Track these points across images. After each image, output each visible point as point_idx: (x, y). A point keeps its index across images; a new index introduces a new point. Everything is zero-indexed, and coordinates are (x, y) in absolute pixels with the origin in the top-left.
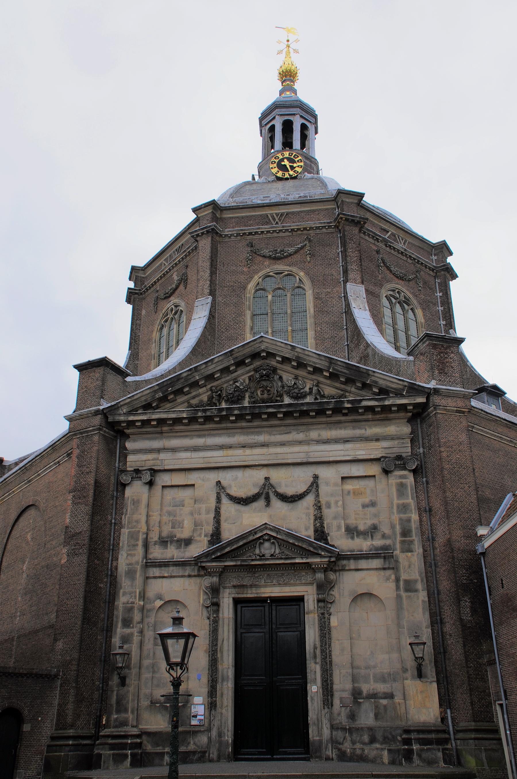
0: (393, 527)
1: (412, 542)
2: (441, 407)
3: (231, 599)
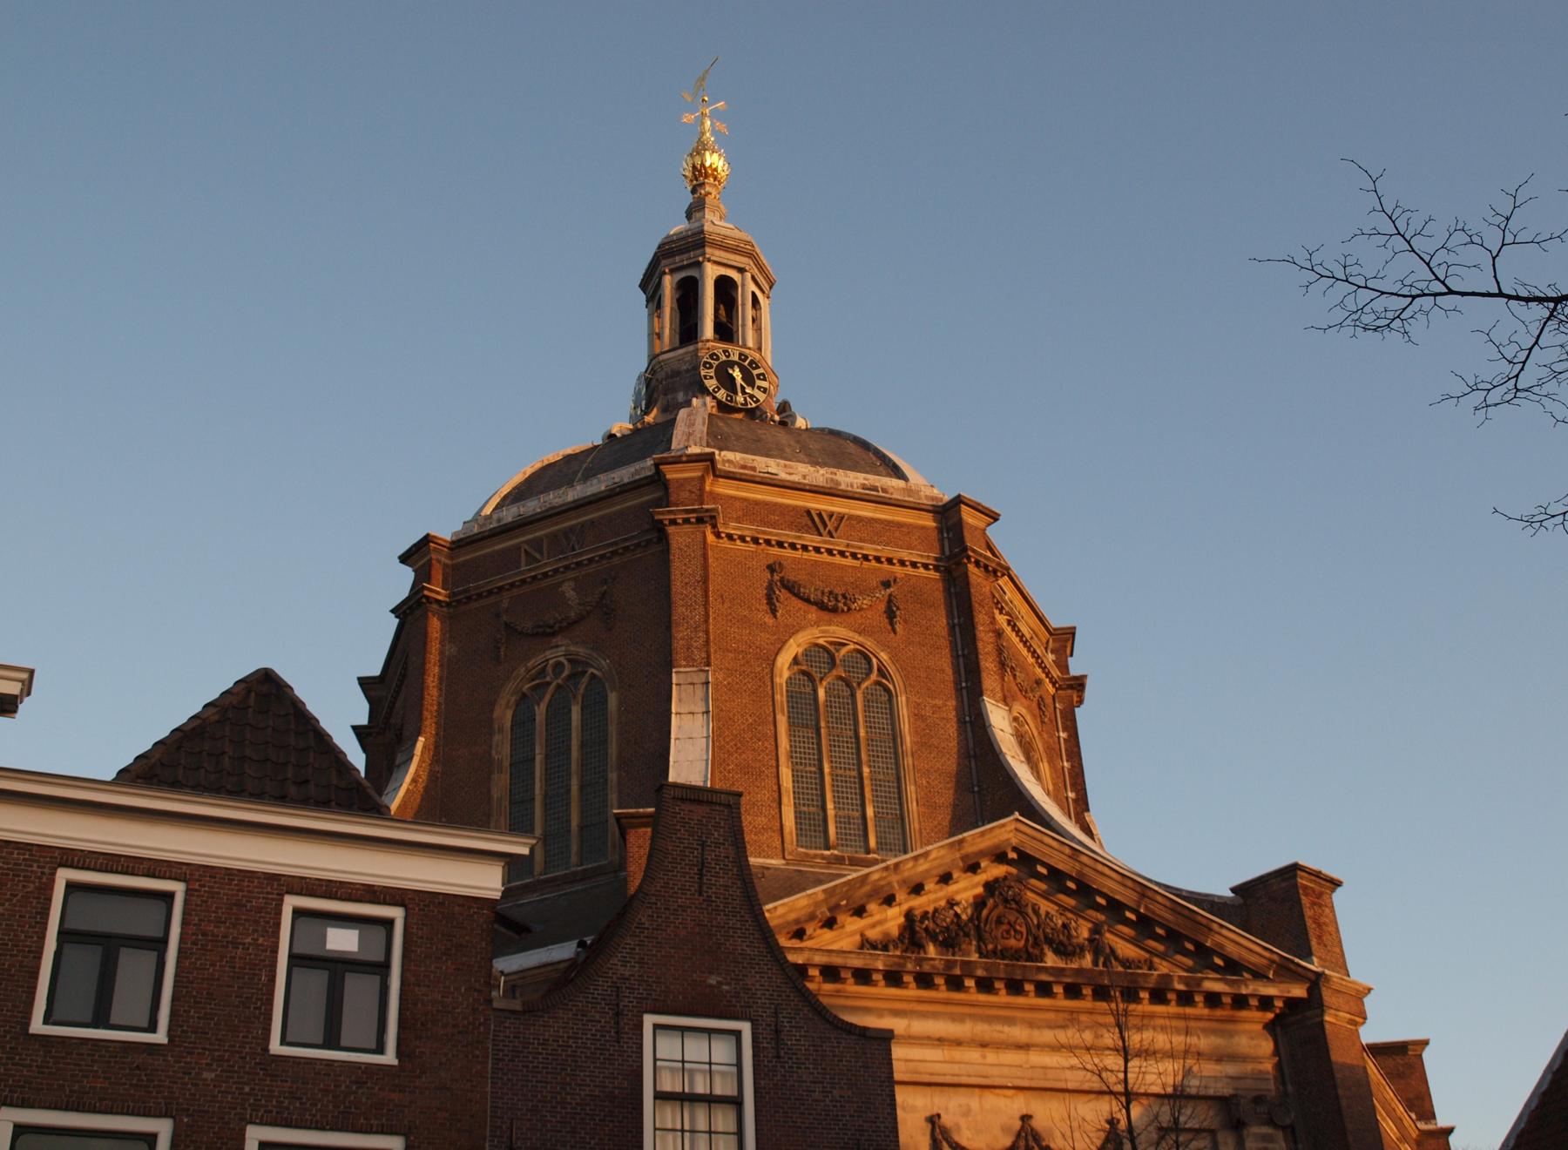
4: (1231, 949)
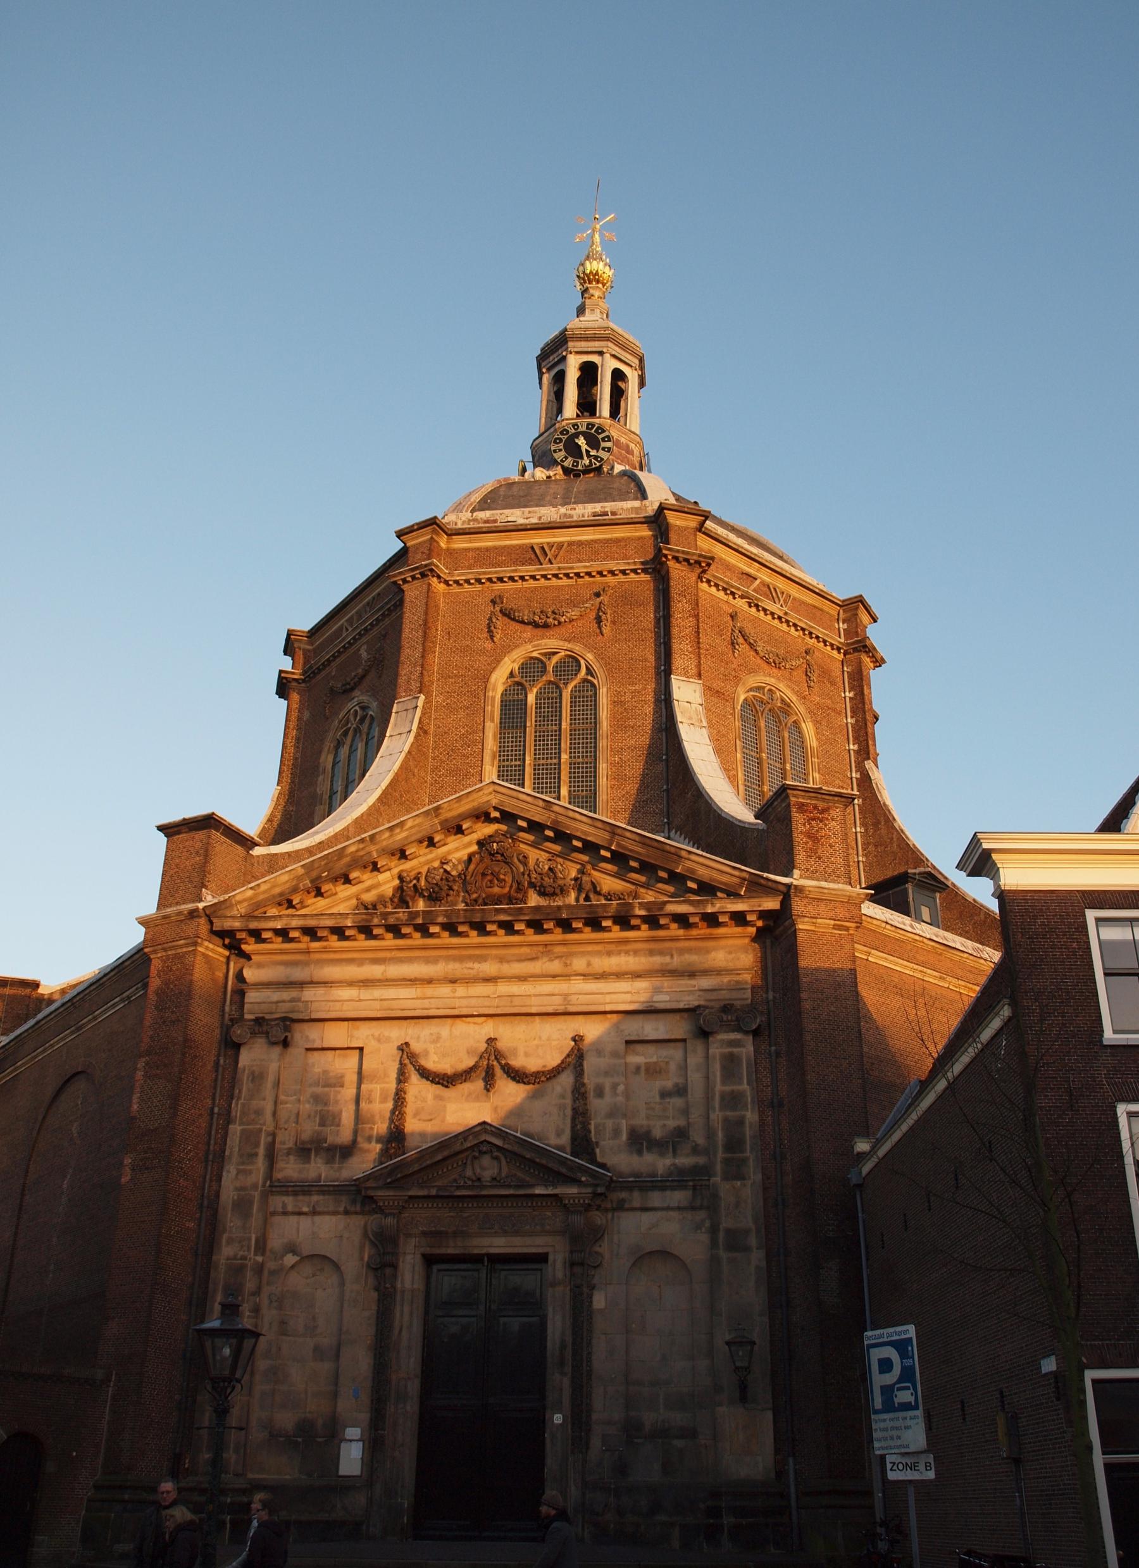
0: (710, 1135)
1: (744, 1161)
2: (806, 919)
3: (418, 1257)
4: (703, 873)
